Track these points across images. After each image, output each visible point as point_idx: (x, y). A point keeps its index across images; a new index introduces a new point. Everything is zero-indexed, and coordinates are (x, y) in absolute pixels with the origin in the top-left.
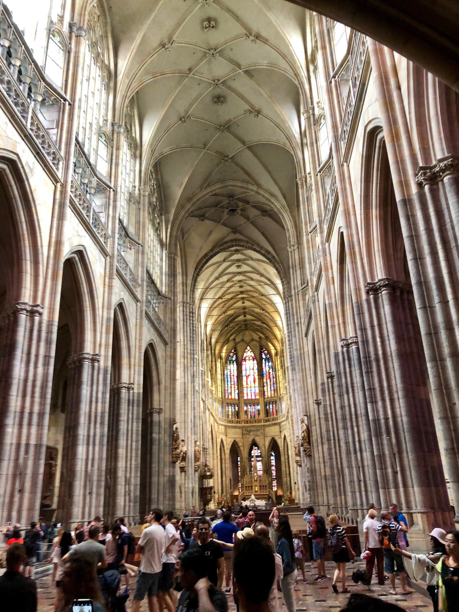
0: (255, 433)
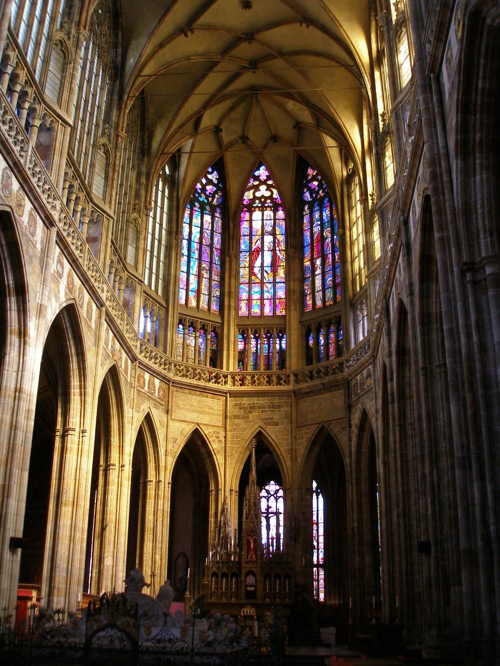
0: (264, 415)
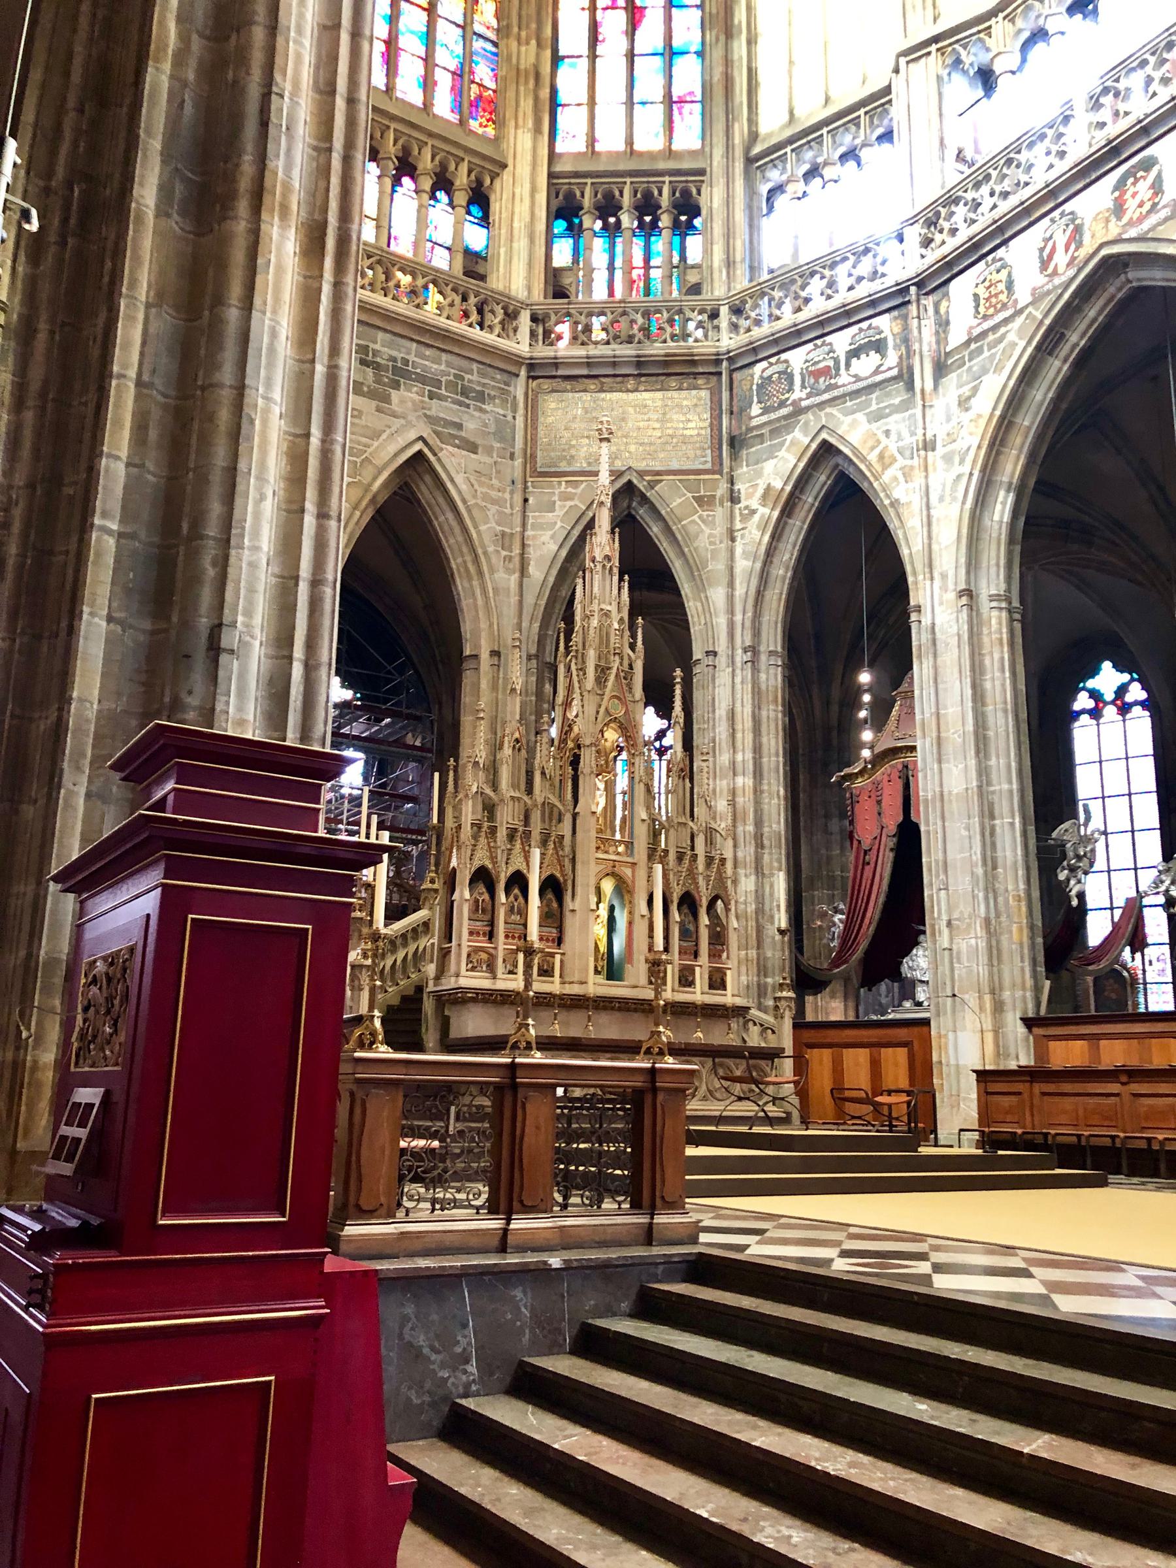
0: (436, 408)
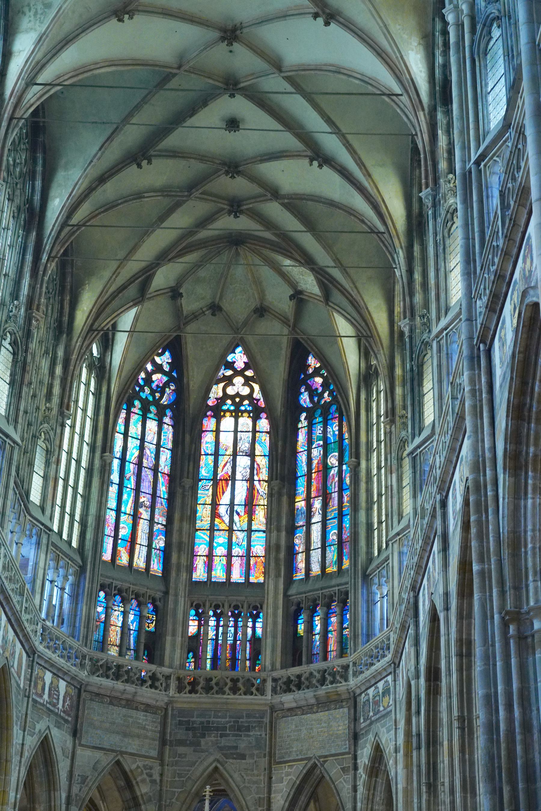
0: (224, 742)
